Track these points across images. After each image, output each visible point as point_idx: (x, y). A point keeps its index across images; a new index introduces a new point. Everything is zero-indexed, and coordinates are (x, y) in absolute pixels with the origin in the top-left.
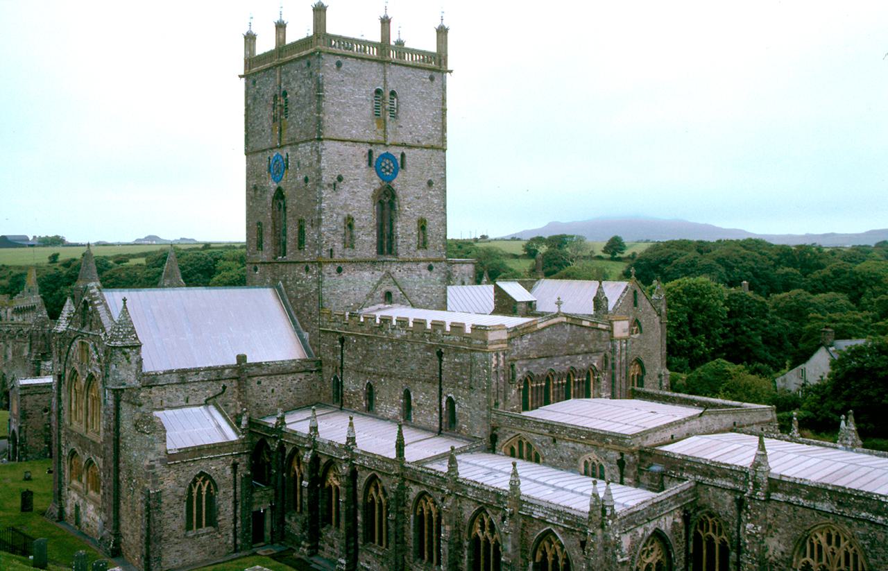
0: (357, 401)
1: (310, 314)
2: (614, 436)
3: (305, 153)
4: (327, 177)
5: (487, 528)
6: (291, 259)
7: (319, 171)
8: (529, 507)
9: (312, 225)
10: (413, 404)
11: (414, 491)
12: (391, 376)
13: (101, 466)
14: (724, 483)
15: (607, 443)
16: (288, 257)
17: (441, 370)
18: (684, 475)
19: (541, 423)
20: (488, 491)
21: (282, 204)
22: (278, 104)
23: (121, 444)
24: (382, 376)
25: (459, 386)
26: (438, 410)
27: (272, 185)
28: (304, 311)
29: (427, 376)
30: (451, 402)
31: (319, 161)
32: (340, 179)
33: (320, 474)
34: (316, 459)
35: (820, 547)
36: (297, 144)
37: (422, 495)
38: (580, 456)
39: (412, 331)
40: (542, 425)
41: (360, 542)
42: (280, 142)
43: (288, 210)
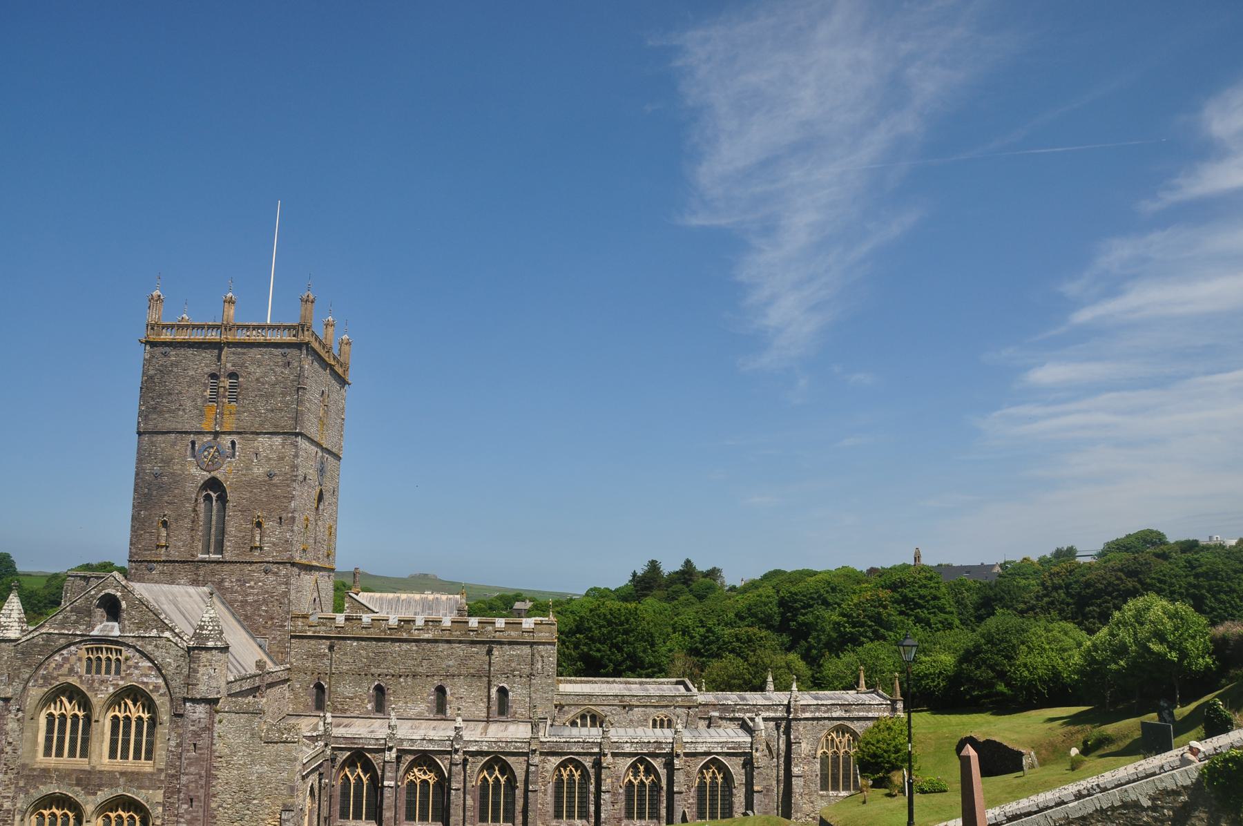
0: (357, 705)
1: (272, 619)
2: (682, 696)
3: (270, 445)
4: (301, 472)
6: (236, 559)
7: (294, 467)
8: (693, 746)
10: (449, 697)
11: (555, 761)
14: (767, 714)
15: (677, 702)
16: (228, 556)
17: (490, 663)
19: (611, 695)
20: (649, 742)
21: (214, 495)
23: (215, 764)
24: (400, 676)
25: (514, 676)
28: (260, 616)
29: (472, 671)
30: (503, 692)
31: (296, 456)
32: (305, 478)
33: (401, 772)
34: (398, 758)
35: (833, 740)
36: (258, 434)
37: (563, 765)
38: (649, 718)
39: (449, 630)
40: (610, 697)
42: (221, 426)
43: (230, 505)
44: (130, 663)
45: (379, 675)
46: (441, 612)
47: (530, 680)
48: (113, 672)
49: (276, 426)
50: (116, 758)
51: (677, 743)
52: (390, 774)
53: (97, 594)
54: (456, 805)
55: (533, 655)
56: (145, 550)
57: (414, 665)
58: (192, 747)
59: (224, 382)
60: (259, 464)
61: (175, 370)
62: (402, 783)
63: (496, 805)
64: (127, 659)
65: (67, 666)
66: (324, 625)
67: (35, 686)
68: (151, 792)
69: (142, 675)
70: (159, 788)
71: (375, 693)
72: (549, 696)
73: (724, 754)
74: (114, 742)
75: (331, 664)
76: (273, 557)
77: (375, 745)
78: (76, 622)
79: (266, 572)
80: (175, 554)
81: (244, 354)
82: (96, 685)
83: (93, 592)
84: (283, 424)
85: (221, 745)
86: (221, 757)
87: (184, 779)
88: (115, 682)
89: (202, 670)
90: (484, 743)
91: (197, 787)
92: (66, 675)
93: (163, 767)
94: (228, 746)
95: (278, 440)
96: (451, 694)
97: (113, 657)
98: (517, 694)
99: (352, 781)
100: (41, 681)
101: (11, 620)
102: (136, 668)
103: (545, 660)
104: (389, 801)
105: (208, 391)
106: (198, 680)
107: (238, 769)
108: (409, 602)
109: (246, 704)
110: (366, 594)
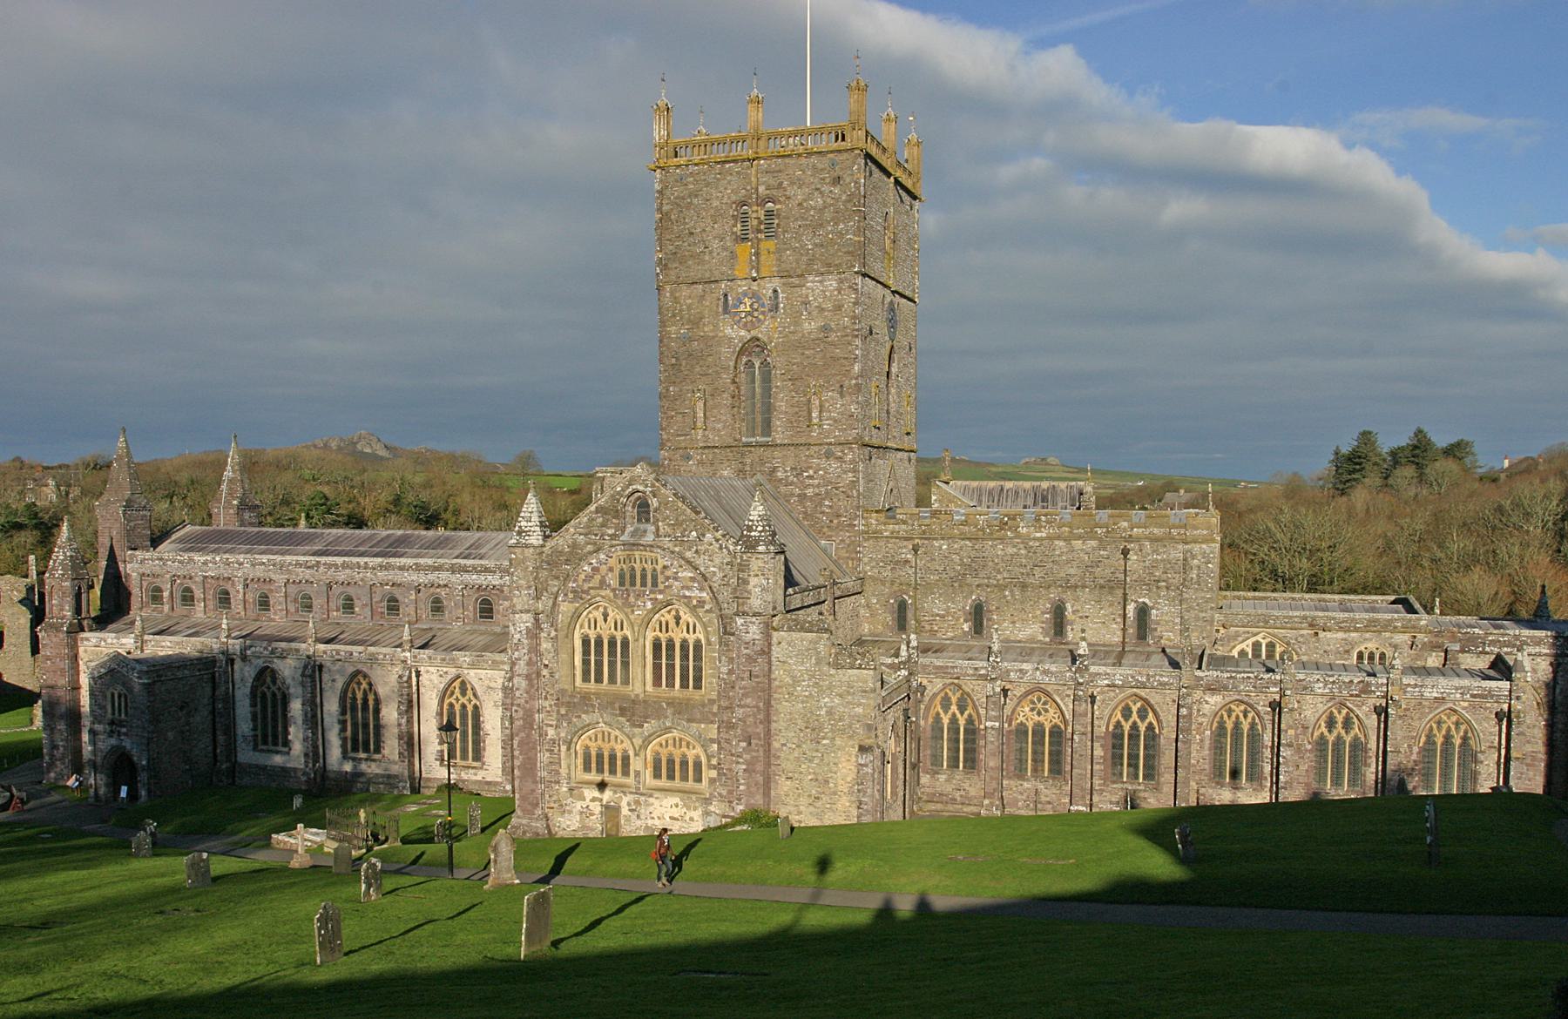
1: (839, 516)
3: (822, 291)
5: (1339, 725)
9: (842, 396)
12: (1024, 586)
13: (714, 734)
15: (1396, 627)
17: (1125, 570)
18: (1487, 649)
22: (754, 215)
23: (775, 696)
25: (1158, 588)
26: (1119, 620)
27: (738, 334)
28: (823, 512)
29: (1102, 581)
30: (1143, 612)
41: (1096, 782)
42: (758, 272)
44: (668, 573)
45: (978, 586)
46: (1060, 504)
47: (1181, 595)
48: (649, 584)
49: (829, 265)
50: (660, 685)
51: (1392, 684)
52: (993, 713)
53: (623, 490)
54: (1081, 756)
55: (1185, 560)
56: (678, 435)
57: (1023, 574)
58: (747, 674)
59: (757, 211)
60: (810, 318)
61: (695, 201)
62: (1010, 725)
63: (1133, 757)
64: (665, 567)
65: (598, 577)
66: (904, 522)
67: (563, 601)
68: (703, 726)
69: (683, 588)
70: (712, 722)
71: (973, 611)
72: (1207, 615)
73: (1466, 704)
74: (657, 668)
75: (916, 573)
76: (835, 436)
77: (973, 675)
78: (603, 525)
79: (828, 455)
80: (714, 439)
81: (780, 171)
82: (632, 599)
83: (619, 489)
84: (837, 262)
85: (782, 672)
86: (780, 687)
87: (740, 712)
88: (652, 596)
89: (753, 581)
90: (1118, 677)
91: (755, 723)
92: (600, 588)
93: (715, 697)
94: (790, 673)
95: (832, 283)
96: (1074, 612)
97: (649, 567)
98: (1163, 613)
99: (946, 721)
100: (571, 596)
101: (532, 524)
102: (676, 579)
103: (1203, 566)
104: (992, 747)
105: (739, 225)
106: (749, 593)
107: (803, 702)
108: (1017, 493)
109: (809, 622)
110: (959, 483)
